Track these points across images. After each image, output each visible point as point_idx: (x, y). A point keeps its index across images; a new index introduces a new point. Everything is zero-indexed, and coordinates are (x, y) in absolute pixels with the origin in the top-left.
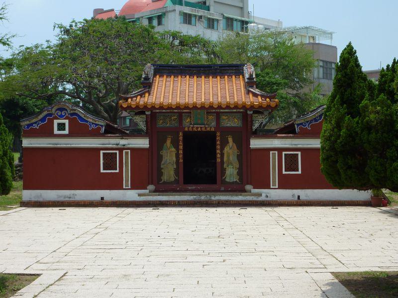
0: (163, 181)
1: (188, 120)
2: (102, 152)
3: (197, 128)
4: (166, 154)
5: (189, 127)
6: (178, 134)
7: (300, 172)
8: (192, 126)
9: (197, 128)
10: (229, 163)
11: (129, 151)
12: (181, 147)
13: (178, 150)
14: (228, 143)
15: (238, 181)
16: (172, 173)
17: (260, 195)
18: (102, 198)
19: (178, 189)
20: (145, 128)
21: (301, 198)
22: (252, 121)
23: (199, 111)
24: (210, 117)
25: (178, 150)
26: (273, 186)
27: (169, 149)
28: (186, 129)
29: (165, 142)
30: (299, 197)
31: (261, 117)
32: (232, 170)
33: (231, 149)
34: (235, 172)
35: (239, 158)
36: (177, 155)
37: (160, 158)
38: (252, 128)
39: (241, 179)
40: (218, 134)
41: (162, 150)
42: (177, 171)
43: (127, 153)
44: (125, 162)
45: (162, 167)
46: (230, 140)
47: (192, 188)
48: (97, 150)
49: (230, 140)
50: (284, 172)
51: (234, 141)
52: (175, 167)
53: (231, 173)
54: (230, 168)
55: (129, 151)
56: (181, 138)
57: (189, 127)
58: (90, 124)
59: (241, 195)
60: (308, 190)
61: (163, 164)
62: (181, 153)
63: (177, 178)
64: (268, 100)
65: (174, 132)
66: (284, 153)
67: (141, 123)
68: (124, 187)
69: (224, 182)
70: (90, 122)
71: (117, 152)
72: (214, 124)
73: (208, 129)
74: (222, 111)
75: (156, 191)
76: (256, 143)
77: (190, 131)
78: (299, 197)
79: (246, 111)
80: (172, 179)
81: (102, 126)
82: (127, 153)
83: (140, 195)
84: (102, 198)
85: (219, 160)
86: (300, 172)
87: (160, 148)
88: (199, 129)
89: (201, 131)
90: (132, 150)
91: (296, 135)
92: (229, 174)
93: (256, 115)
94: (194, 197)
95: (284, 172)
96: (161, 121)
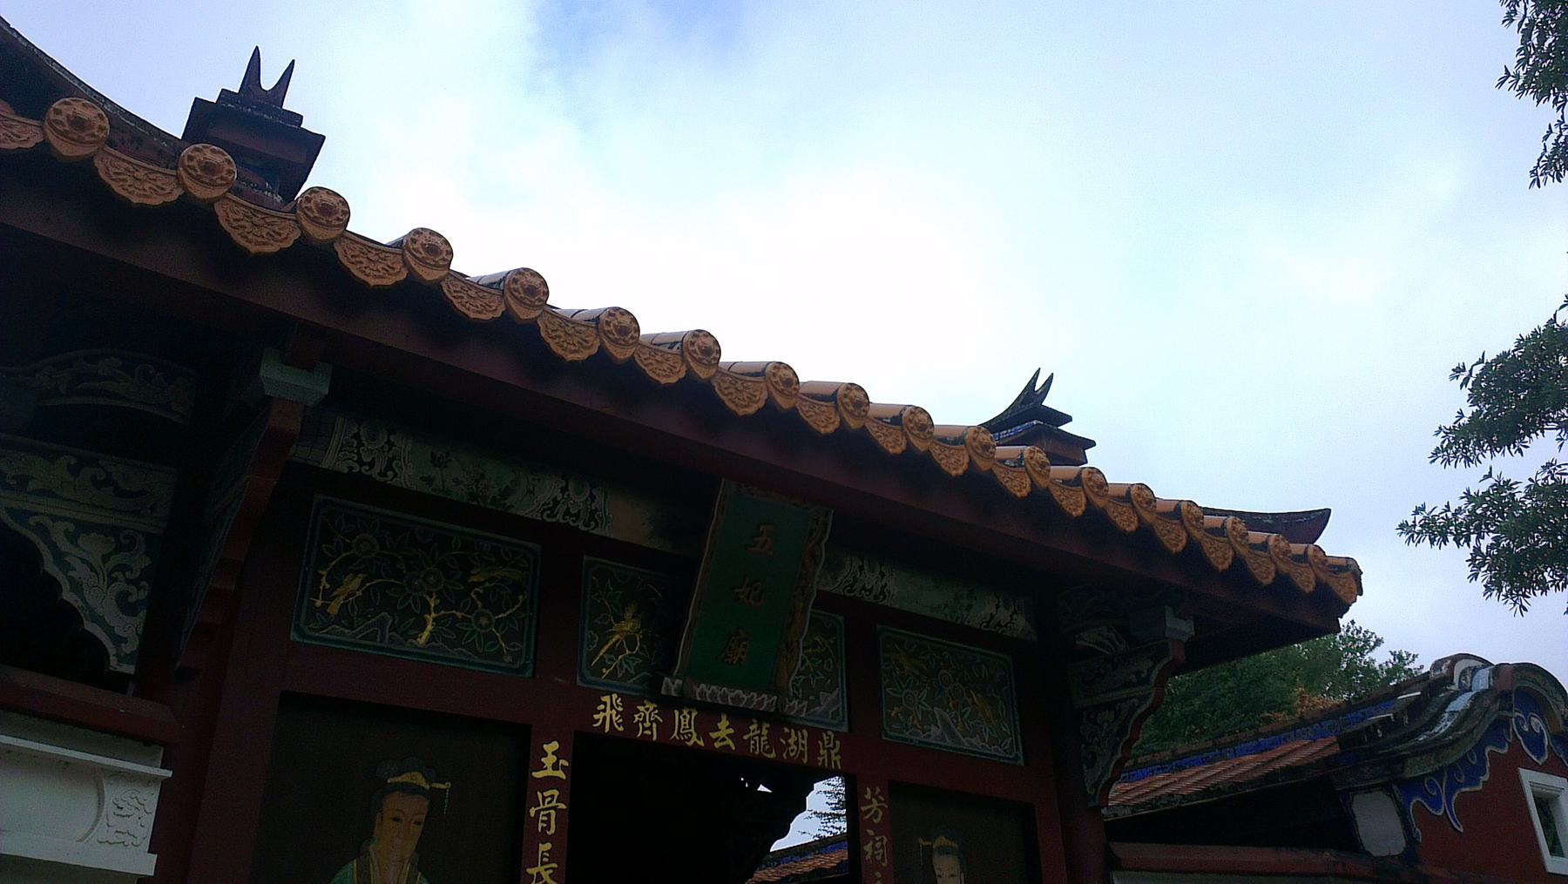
6: (528, 758)
20: (129, 628)
28: (608, 714)
56: (548, 808)
67: (93, 547)
74: (899, 589)
96: (353, 584)
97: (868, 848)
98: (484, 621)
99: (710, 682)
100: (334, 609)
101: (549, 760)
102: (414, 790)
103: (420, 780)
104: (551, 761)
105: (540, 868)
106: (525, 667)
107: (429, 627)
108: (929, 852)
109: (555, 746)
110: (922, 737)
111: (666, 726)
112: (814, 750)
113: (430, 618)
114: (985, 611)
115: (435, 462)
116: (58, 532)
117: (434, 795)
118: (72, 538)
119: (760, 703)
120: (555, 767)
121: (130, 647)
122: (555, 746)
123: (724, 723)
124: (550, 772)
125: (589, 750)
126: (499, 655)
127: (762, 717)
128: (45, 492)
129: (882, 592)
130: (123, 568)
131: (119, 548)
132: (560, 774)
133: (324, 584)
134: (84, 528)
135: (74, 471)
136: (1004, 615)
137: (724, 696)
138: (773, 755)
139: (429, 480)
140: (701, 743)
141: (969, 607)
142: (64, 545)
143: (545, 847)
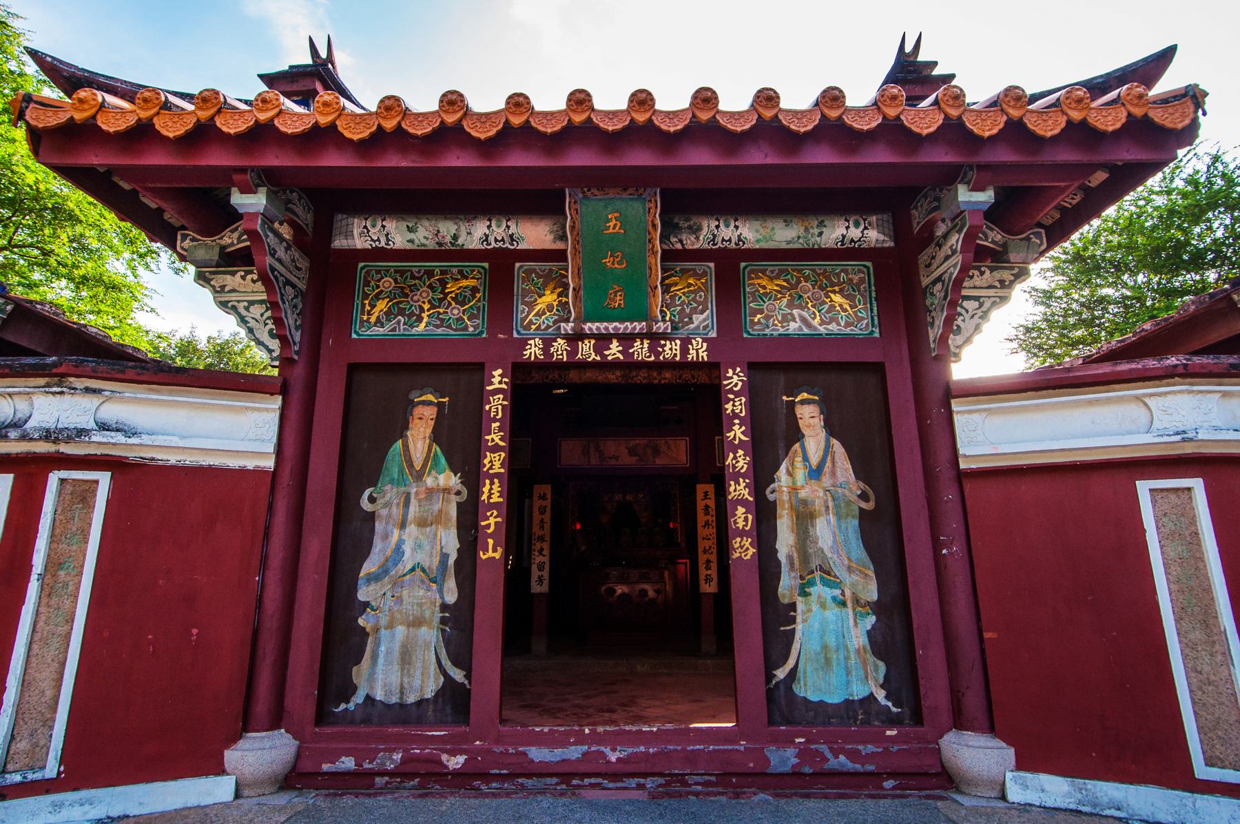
0: (359, 698)
1: (549, 298)
3: (602, 340)
5: (547, 343)
8: (568, 327)
9: (602, 340)
11: (104, 479)
12: (494, 462)
13: (473, 478)
14: (795, 435)
15: (880, 695)
25: (473, 478)
27: (419, 476)
28: (533, 350)
29: (400, 429)
32: (832, 613)
35: (882, 531)
37: (351, 536)
40: (735, 379)
42: (458, 624)
45: (362, 596)
46: (809, 416)
49: (809, 416)
51: (832, 428)
52: (451, 597)
53: (832, 645)
55: (104, 479)
56: (496, 405)
57: (547, 343)
61: (373, 578)
63: (458, 675)
65: (457, 374)
69: (783, 707)
72: (704, 320)
73: (671, 350)
76: (983, 437)
80: (425, 683)
85: (744, 549)
87: (361, 461)
88: (614, 350)
89: (629, 365)
92: (814, 646)
96: (382, 305)
97: (729, 406)
98: (456, 312)
99: (593, 321)
100: (373, 319)
101: (496, 380)
102: (429, 403)
103: (430, 397)
104: (497, 380)
105: (493, 436)
106: (482, 332)
107: (425, 320)
108: (792, 405)
109: (500, 371)
110: (781, 331)
111: (573, 352)
112: (684, 351)
113: (424, 315)
114: (836, 232)
115: (410, 230)
116: (241, 307)
117: (440, 406)
118: (247, 309)
119: (635, 328)
120: (500, 383)
122: (500, 371)
123: (615, 343)
125: (520, 371)
127: (642, 336)
128: (234, 291)
129: (740, 240)
132: (504, 386)
133: (368, 308)
135: (243, 278)
136: (855, 233)
137: (606, 328)
138: (653, 358)
139: (411, 241)
140: (598, 358)
141: (820, 234)
142: (244, 312)
143: (495, 425)
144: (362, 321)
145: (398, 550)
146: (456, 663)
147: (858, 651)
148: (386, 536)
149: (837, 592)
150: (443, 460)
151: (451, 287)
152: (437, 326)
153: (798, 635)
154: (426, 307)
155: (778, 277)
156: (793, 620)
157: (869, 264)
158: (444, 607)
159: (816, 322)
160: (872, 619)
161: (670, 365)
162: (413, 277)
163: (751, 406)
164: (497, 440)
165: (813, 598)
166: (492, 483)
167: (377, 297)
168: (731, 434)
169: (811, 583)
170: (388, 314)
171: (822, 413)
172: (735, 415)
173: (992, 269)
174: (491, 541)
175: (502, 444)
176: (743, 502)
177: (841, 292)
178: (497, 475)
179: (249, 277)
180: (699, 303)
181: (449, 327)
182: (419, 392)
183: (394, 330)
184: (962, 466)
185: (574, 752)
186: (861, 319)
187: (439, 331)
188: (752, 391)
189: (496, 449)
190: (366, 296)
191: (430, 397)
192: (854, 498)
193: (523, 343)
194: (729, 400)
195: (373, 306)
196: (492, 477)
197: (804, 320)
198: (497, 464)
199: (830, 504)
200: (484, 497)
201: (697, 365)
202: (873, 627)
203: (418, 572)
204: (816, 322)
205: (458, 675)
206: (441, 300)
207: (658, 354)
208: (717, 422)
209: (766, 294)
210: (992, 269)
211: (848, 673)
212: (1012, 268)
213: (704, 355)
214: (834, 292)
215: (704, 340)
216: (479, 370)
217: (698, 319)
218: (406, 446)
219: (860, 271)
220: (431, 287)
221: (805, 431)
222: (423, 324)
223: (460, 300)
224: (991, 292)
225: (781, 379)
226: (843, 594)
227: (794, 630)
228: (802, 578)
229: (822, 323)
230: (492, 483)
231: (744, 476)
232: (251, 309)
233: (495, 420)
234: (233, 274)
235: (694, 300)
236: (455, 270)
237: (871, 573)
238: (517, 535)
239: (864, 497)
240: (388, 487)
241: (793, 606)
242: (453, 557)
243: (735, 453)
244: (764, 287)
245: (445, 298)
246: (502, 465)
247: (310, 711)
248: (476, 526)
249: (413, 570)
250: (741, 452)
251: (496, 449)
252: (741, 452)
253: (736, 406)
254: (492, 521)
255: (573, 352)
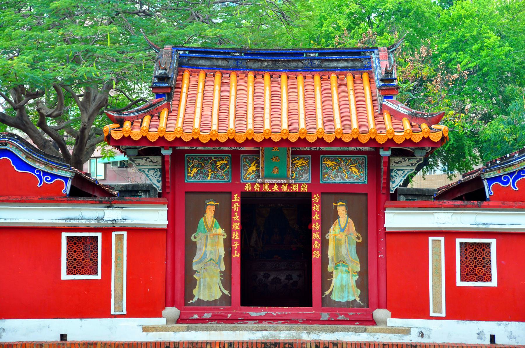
0: (195, 299)
1: (253, 168)
2: (64, 235)
3: (271, 185)
4: (204, 241)
5: (253, 185)
6: (232, 198)
7: (494, 283)
8: (260, 181)
9: (271, 185)
10: (340, 262)
11: (125, 233)
12: (236, 226)
13: (229, 231)
14: (337, 217)
15: (358, 300)
16: (217, 281)
17: (407, 331)
18: (63, 337)
19: (229, 316)
20: (160, 185)
21: (498, 341)
22: (389, 171)
23: (275, 149)
24: (299, 163)
25: (229, 231)
26: (434, 312)
27: (210, 230)
28: (248, 188)
29: (202, 213)
30: (493, 338)
31: (408, 162)
32: (345, 276)
33: (342, 230)
34: (352, 280)
35: (362, 250)
36: (228, 243)
37: (191, 249)
38: (388, 188)
39: (365, 295)
40: (316, 198)
41: (195, 232)
43: (120, 238)
44: (116, 258)
45: (194, 268)
46: (342, 211)
47: (259, 314)
48: (54, 231)
49: (342, 211)
50: (459, 283)
51: (349, 215)
52: (223, 268)
53: (343, 284)
54: (342, 272)
55: (125, 233)
56: (236, 207)
57: (253, 185)
58: (39, 176)
59: (365, 331)
60: (514, 323)
62: (237, 238)
63: (226, 292)
64: (424, 126)
65: (220, 192)
66: (458, 241)
68: (112, 312)
69: (326, 302)
70: (39, 171)
71: (99, 235)
72: (307, 177)
73: (295, 188)
75: (180, 320)
76: (396, 219)
77: (257, 192)
78: (493, 338)
79: (377, 150)
81: (66, 179)
82: (120, 238)
83: (145, 329)
84: (63, 337)
85: (316, 255)
86: (494, 283)
88: (275, 188)
89: (281, 193)
90: (134, 231)
91: (485, 203)
92: (338, 284)
93: (398, 159)
94: (265, 333)
95: (459, 283)
96: (194, 170)
97: (314, 208)
100: (192, 175)
101: (236, 198)
102: (212, 205)
107: (210, 175)
108: (336, 206)
109: (237, 195)
110: (334, 181)
111: (262, 188)
112: (300, 188)
116: (146, 171)
117: (216, 205)
118: (148, 172)
121: (160, 188)
122: (237, 195)
124: (236, 200)
126: (224, 179)
128: (143, 165)
130: (156, 175)
131: (155, 172)
133: (190, 171)
134: (149, 169)
135: (146, 160)
138: (289, 191)
143: (236, 213)
144: (188, 176)
145: (205, 254)
146: (226, 289)
147: (352, 286)
148: (200, 249)
149: (347, 268)
150: (218, 225)
151: (218, 163)
152: (214, 178)
153: (333, 282)
154: (210, 171)
155: (333, 161)
156: (332, 277)
157: (366, 156)
158: (221, 272)
159: (346, 178)
160: (358, 277)
161: (295, 193)
162: (205, 160)
163: (321, 208)
164: (237, 218)
165: (339, 270)
166: (236, 233)
167: (193, 167)
168: (314, 217)
169: (338, 266)
170: (197, 173)
171: (346, 209)
172: (316, 211)
173: (409, 159)
174: (236, 252)
175: (238, 220)
176: (317, 240)
177: (355, 167)
178: (237, 230)
179: (148, 160)
180: (305, 170)
181: (218, 178)
182: (208, 201)
183: (199, 179)
184: (387, 230)
185: (263, 313)
186: (361, 177)
187: (215, 180)
188: (321, 202)
189: (236, 221)
190: (189, 167)
191: (212, 203)
192: (355, 238)
193: (244, 185)
194: (314, 206)
195: (192, 171)
196: (235, 231)
197: (342, 177)
198: (237, 227)
199: (347, 240)
200: (233, 237)
201: (304, 193)
202: (358, 279)
203: (212, 261)
204: (346, 178)
205: (226, 292)
206: (215, 168)
207: (290, 189)
208: (309, 213)
209: (329, 167)
210: (409, 159)
211: (348, 293)
212: (416, 159)
213: (306, 190)
214: (353, 167)
215: (307, 184)
216: (231, 194)
217: (305, 176)
218: (205, 220)
219: (363, 159)
220: (211, 163)
221: (340, 215)
222: (209, 177)
223: (222, 168)
224: (408, 168)
225: (333, 197)
226: (349, 269)
227: (332, 281)
228: (336, 264)
229: (348, 178)
230: (236, 233)
231: (318, 231)
232: (150, 171)
233: (236, 212)
234: (142, 159)
235: (304, 169)
236: (219, 157)
237: (359, 263)
238: (243, 250)
239: (358, 238)
240: (200, 234)
241: (332, 273)
242: (223, 256)
243: (315, 223)
244: (328, 165)
245: (216, 168)
246: (239, 227)
247: (183, 302)
248: (231, 246)
249: (210, 260)
250: (317, 223)
251: (236, 221)
252: (317, 223)
253: (316, 208)
254: (236, 245)
255: (262, 188)
